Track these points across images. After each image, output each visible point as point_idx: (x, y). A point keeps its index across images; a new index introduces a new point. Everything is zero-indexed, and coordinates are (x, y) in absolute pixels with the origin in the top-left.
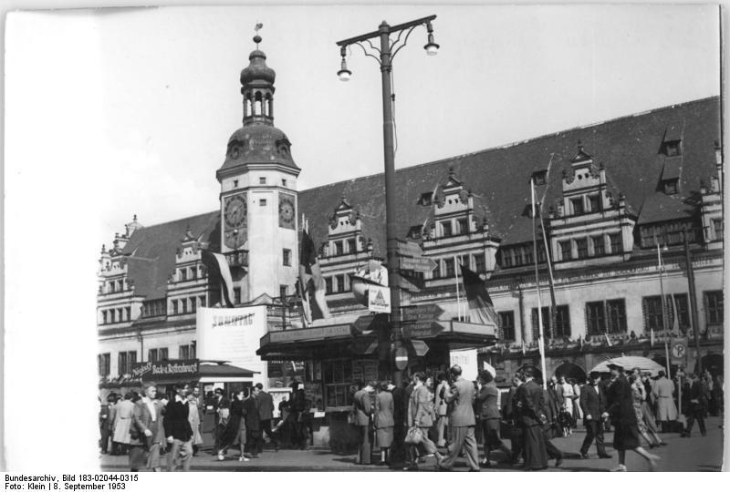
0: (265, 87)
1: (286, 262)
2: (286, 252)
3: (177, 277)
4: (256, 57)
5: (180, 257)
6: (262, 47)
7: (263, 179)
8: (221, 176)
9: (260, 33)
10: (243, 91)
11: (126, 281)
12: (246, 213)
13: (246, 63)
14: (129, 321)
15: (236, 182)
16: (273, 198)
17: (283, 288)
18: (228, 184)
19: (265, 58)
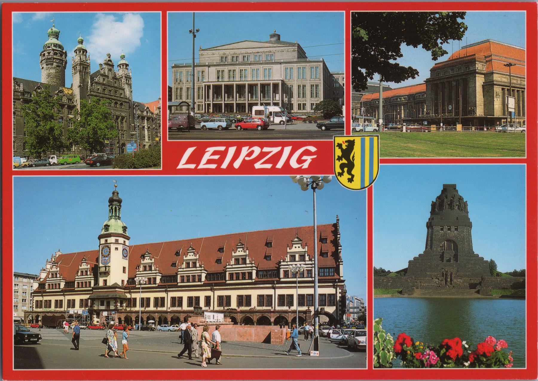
1: (124, 271)
2: (124, 268)
7: (117, 240)
12: (110, 252)
15: (106, 240)
16: (120, 247)
17: (123, 281)
18: (103, 241)
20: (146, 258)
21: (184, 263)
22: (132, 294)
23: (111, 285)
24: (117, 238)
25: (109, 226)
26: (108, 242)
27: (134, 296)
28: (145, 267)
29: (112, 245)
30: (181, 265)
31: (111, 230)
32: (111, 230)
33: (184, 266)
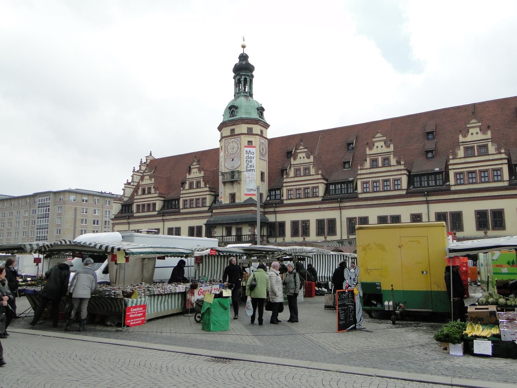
0: (248, 76)
1: (262, 179)
2: (262, 174)
3: (187, 186)
4: (243, 57)
5: (189, 174)
6: (247, 51)
8: (220, 128)
9: (245, 43)
10: (234, 78)
11: (154, 187)
13: (237, 61)
14: (154, 210)
15: (233, 131)
17: (261, 195)
18: (227, 131)
19: (248, 57)
20: (300, 155)
21: (368, 159)
22: (277, 215)
23: (242, 201)
24: (250, 126)
25: (236, 108)
26: (236, 132)
27: (280, 218)
28: (297, 170)
29: (243, 136)
30: (362, 165)
31: (241, 114)
32: (241, 114)
33: (367, 164)
